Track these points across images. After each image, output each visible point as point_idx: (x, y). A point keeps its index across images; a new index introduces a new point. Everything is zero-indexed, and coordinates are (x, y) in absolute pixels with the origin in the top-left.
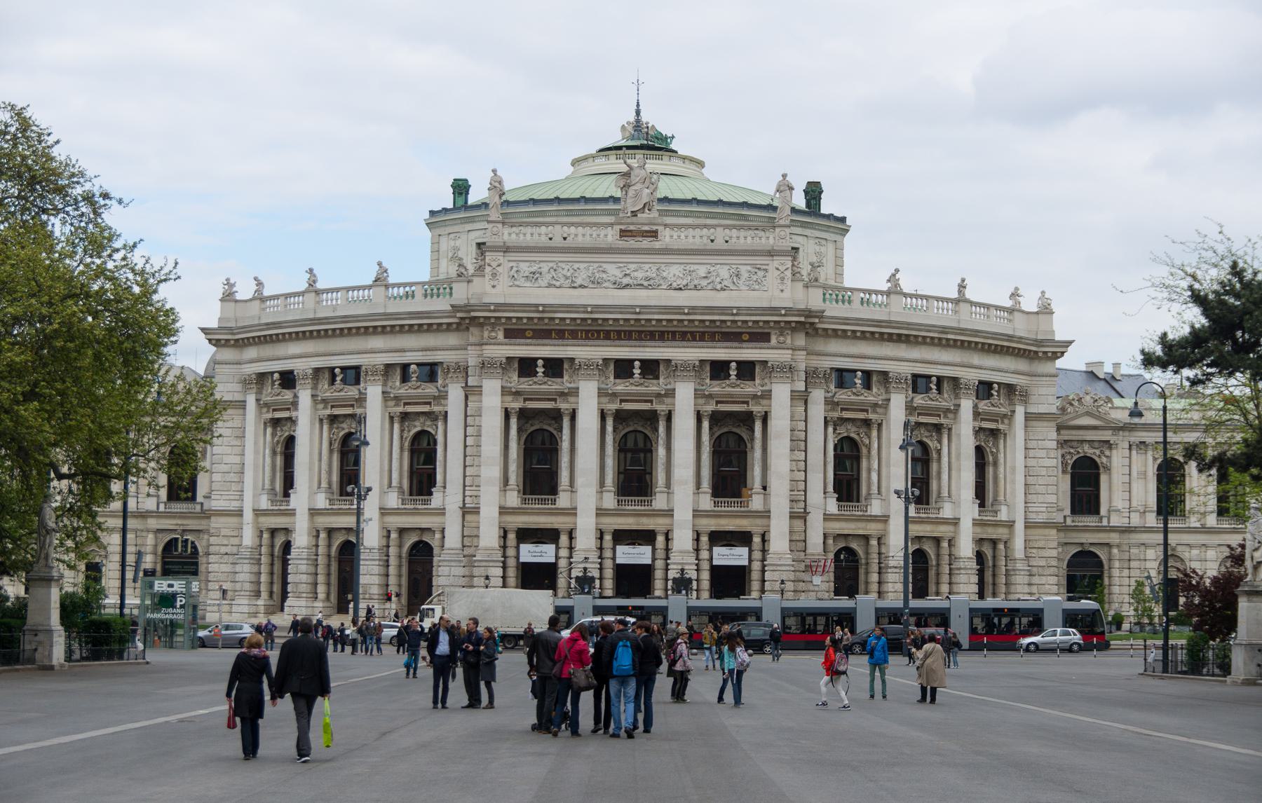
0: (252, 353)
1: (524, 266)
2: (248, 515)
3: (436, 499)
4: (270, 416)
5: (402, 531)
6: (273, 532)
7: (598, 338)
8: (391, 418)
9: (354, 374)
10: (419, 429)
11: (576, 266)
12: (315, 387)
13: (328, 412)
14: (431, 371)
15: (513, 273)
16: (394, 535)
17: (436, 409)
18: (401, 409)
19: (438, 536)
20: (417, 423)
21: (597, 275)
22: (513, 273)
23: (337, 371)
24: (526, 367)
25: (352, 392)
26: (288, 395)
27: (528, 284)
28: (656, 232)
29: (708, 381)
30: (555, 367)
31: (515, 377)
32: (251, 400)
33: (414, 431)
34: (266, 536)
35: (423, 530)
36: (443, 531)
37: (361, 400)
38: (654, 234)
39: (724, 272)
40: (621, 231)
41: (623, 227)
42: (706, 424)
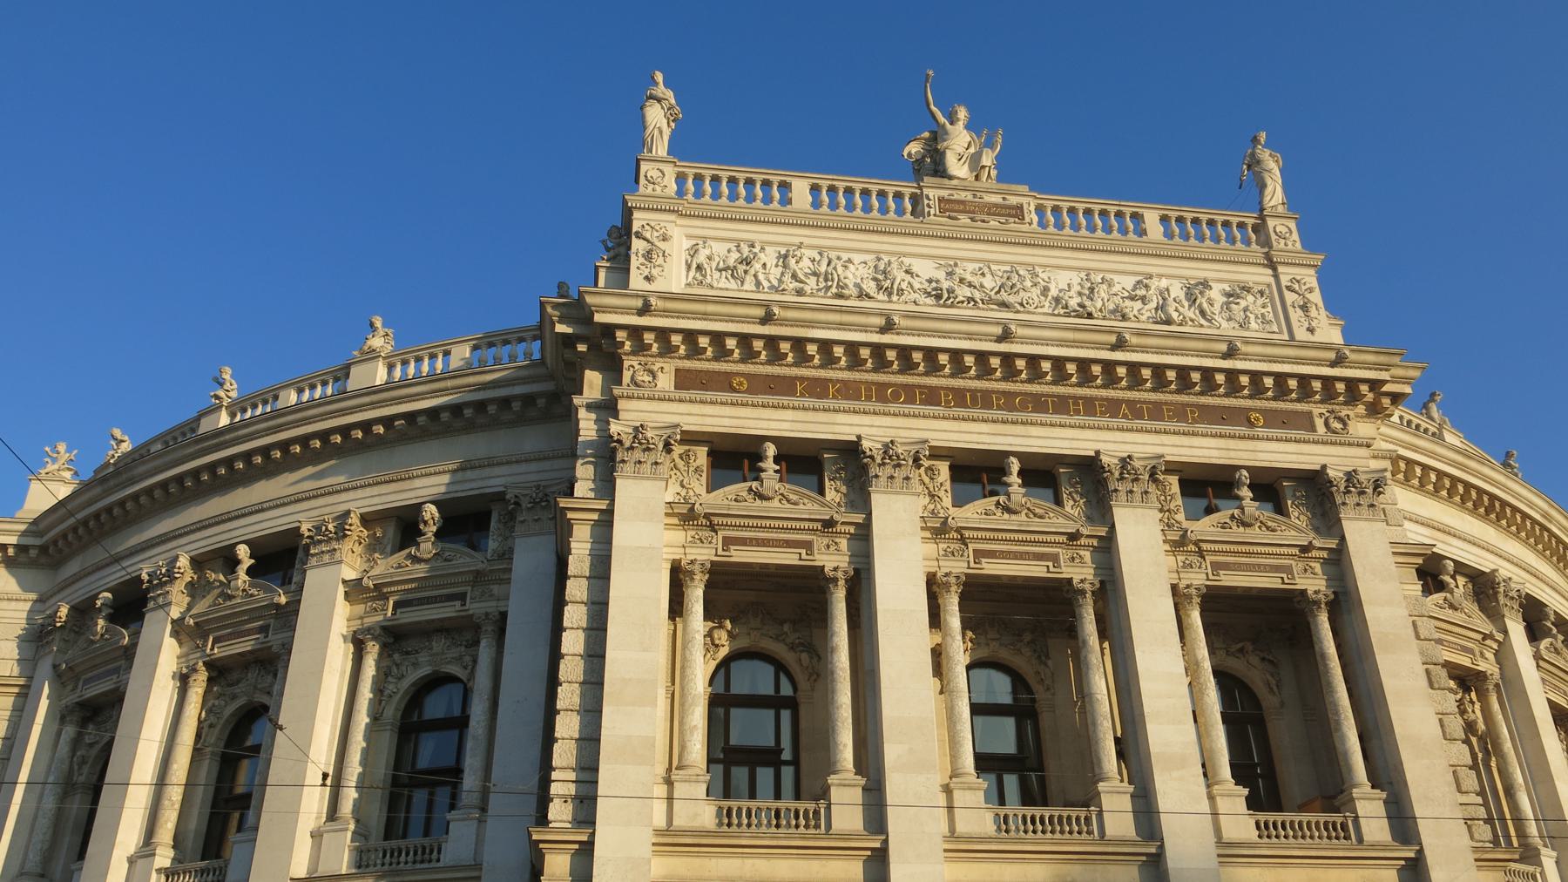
0: (73, 567)
1: (719, 249)
4: (73, 698)
7: (910, 400)
10: (425, 670)
11: (845, 256)
15: (701, 258)
17: (476, 607)
20: (423, 658)
21: (900, 275)
22: (701, 258)
23: (243, 551)
24: (732, 458)
27: (733, 284)
28: (1020, 208)
29: (1181, 517)
30: (803, 461)
31: (699, 486)
33: (414, 676)
38: (1018, 212)
39: (1177, 291)
40: (941, 200)
41: (945, 193)
42: (1195, 618)
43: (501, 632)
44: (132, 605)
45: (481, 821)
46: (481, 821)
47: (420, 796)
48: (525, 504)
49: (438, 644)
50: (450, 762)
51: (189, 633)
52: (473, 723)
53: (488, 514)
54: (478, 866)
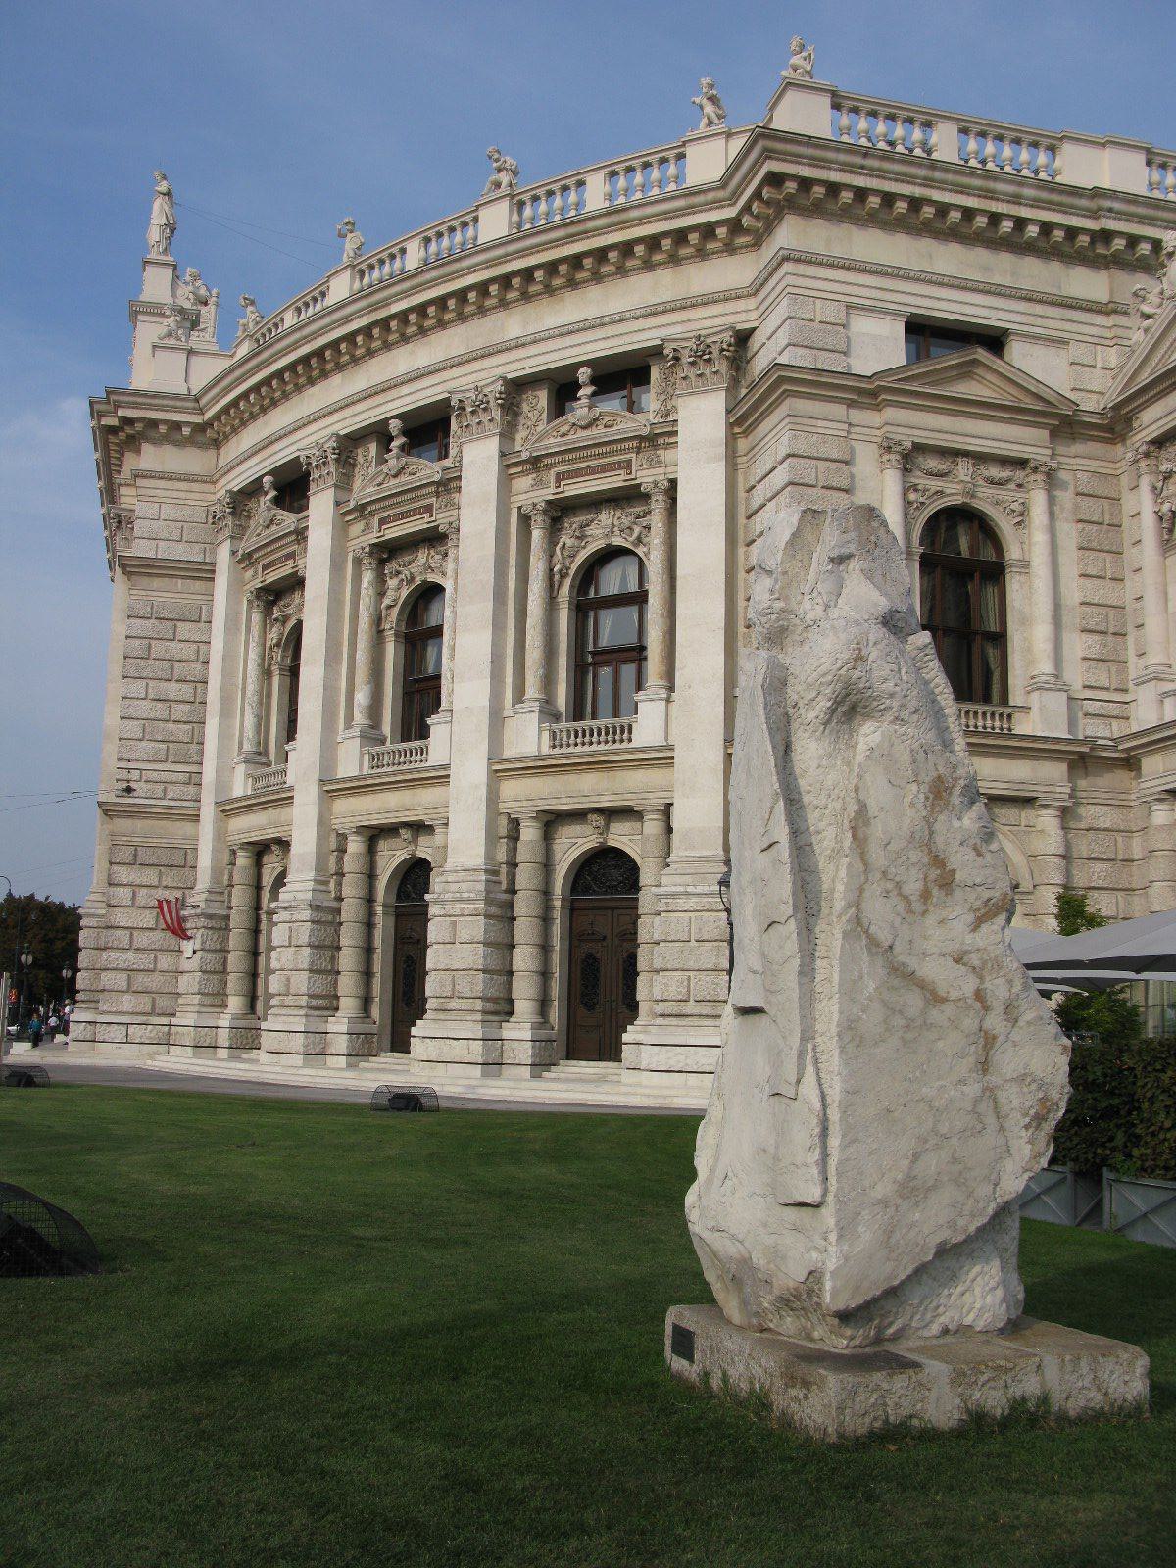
2: (208, 812)
3: (648, 725)
5: (552, 821)
6: (260, 850)
8: (525, 520)
9: (428, 429)
12: (344, 484)
13: (373, 538)
14: (623, 375)
16: (529, 833)
17: (646, 476)
18: (548, 493)
19: (652, 826)
23: (395, 426)
25: (427, 469)
26: (288, 520)
32: (223, 556)
34: (243, 860)
35: (612, 814)
36: (667, 810)
37: (448, 485)
43: (674, 500)
44: (292, 487)
45: (668, 700)
46: (668, 700)
47: (606, 672)
48: (686, 359)
49: (605, 517)
50: (631, 639)
51: (351, 513)
52: (651, 600)
53: (648, 368)
54: (671, 748)
